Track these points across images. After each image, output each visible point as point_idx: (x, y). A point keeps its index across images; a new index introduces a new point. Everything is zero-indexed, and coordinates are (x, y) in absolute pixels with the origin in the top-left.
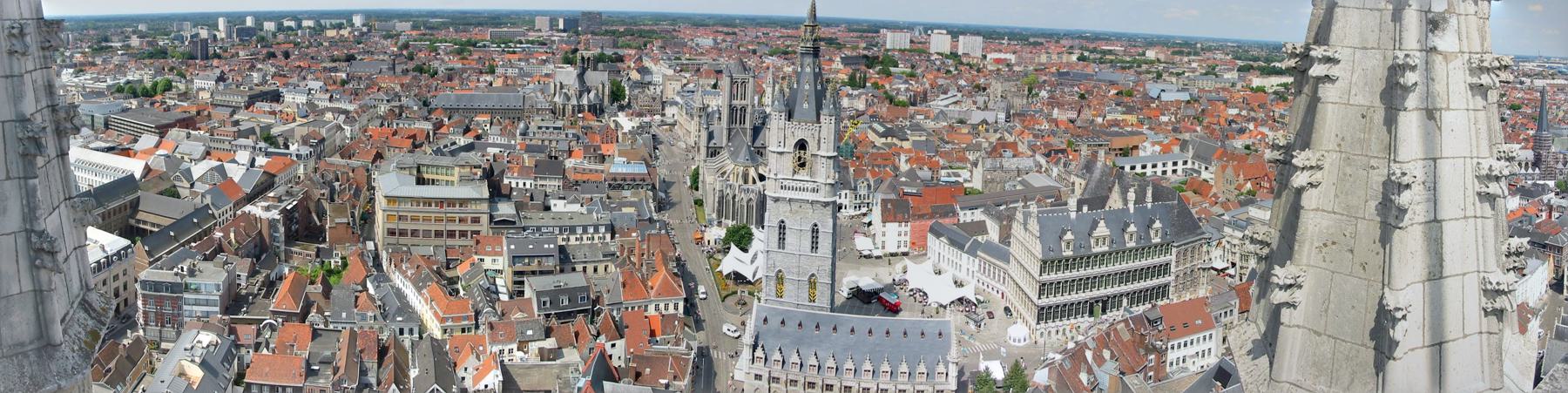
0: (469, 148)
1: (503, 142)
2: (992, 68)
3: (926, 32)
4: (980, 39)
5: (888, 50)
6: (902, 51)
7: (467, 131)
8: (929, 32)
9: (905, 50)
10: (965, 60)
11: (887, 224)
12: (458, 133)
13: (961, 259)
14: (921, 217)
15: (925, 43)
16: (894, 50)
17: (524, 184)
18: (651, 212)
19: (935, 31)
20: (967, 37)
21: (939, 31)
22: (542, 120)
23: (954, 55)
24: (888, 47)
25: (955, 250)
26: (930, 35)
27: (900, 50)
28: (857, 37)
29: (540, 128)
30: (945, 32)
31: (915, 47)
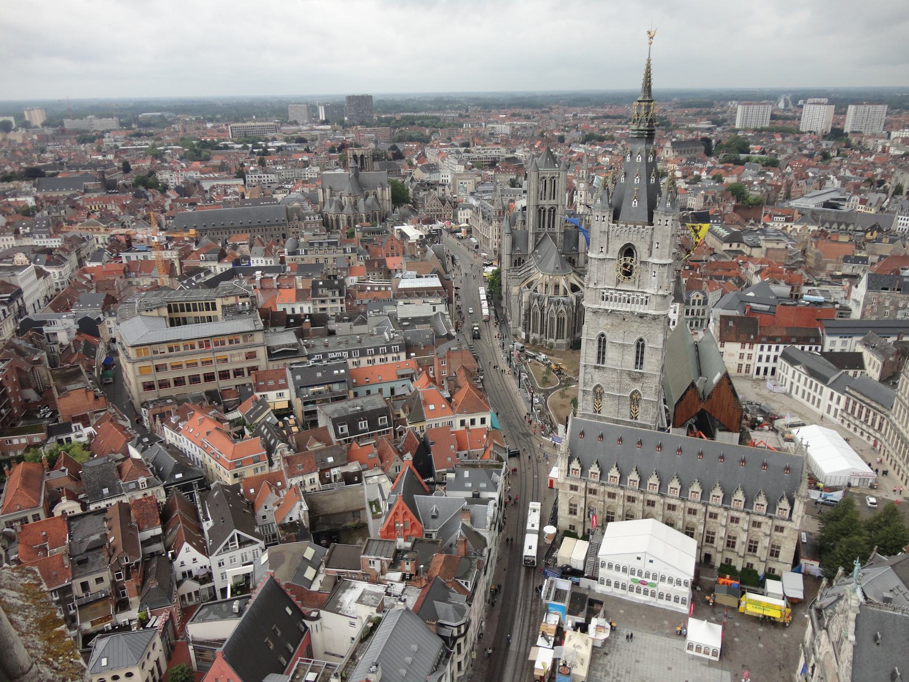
0: (228, 275)
1: (269, 264)
2: (898, 153)
3: (795, 102)
4: (882, 109)
5: (737, 131)
6: (759, 131)
7: (221, 256)
8: (800, 102)
9: (762, 130)
10: (854, 140)
11: (727, 345)
12: (212, 260)
13: (821, 394)
14: (771, 340)
15: (793, 118)
16: (746, 130)
17: (301, 309)
18: (448, 328)
19: (810, 100)
20: (861, 108)
21: (816, 100)
22: (314, 235)
23: (836, 134)
24: (737, 126)
25: (815, 382)
26: (801, 107)
27: (755, 130)
28: (695, 115)
29: (312, 244)
30: (825, 100)
31: (780, 123)
